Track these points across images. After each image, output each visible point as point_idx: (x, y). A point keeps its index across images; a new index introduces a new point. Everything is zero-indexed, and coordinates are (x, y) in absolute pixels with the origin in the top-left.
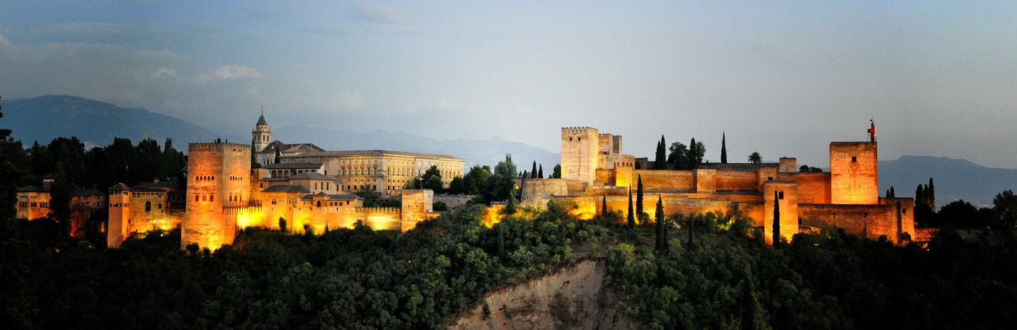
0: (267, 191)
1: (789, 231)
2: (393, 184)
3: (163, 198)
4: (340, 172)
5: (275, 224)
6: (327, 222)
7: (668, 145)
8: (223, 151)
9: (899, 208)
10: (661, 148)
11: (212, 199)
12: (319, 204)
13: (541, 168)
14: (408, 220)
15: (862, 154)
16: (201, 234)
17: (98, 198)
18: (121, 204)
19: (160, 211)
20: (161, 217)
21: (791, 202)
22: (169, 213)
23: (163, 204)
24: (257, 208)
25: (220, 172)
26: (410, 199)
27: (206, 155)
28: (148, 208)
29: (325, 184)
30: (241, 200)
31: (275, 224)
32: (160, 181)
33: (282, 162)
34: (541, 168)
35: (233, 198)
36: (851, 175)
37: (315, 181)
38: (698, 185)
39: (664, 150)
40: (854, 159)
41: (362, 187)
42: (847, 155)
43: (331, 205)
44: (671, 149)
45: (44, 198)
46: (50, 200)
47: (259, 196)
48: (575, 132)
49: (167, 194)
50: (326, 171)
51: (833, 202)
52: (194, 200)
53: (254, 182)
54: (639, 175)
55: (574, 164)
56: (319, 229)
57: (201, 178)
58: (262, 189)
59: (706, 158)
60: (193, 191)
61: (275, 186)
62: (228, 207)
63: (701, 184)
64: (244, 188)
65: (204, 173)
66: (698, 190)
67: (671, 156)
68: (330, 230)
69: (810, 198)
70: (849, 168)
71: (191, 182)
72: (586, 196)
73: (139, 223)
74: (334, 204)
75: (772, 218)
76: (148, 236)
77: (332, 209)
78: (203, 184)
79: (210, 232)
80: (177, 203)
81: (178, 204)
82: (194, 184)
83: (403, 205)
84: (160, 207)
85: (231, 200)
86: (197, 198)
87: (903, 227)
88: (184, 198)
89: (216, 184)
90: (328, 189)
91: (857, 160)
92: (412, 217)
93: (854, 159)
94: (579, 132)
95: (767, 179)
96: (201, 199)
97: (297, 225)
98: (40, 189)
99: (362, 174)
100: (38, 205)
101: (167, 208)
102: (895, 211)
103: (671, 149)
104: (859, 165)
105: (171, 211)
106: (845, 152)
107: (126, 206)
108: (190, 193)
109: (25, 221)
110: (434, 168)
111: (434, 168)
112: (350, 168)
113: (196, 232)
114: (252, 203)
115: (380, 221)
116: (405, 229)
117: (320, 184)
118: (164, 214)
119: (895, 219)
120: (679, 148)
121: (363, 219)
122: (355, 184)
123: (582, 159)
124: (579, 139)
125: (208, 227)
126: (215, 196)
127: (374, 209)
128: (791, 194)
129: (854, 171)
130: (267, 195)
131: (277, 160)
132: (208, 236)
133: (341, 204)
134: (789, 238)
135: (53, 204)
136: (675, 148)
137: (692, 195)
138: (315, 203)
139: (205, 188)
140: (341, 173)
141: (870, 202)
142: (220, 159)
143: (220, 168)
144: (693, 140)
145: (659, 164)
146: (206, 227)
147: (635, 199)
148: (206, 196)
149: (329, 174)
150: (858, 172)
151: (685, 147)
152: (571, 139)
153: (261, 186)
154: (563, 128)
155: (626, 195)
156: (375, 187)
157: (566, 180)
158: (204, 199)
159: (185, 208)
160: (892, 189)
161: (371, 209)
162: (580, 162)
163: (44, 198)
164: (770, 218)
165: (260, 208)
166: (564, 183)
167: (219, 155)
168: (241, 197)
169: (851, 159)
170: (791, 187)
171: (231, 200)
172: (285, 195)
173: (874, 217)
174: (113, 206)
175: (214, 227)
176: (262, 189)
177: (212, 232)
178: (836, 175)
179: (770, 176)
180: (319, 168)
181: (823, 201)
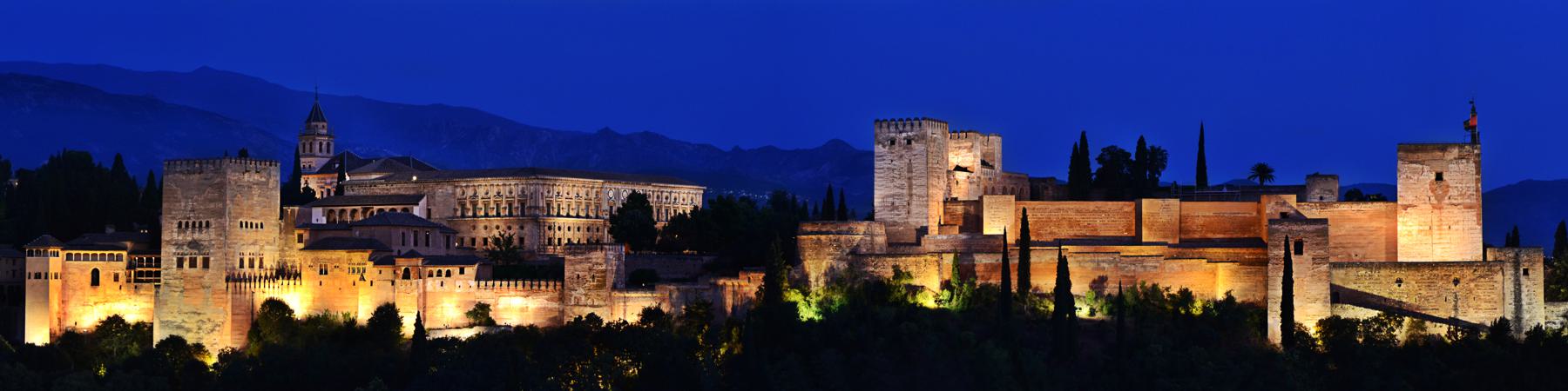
0: (310, 247)
1: (1310, 314)
2: (558, 234)
3: (120, 267)
4: (455, 210)
7: (1094, 153)
8: (225, 173)
9: (1517, 270)
10: (1080, 156)
13: (842, 195)
14: (577, 304)
15: (1453, 166)
17: (14, 264)
18: (47, 275)
19: (117, 285)
20: (118, 298)
21: (1316, 260)
22: (133, 290)
23: (122, 274)
24: (292, 282)
25: (220, 214)
26: (580, 262)
28: (95, 280)
29: (422, 236)
32: (116, 230)
33: (348, 192)
34: (842, 195)
36: (1434, 207)
37: (401, 230)
38: (1145, 232)
39: (1087, 163)
40: (1439, 177)
41: (496, 241)
42: (1426, 168)
43: (431, 275)
44: (1100, 160)
47: (297, 256)
48: (901, 129)
50: (429, 211)
51: (1399, 260)
52: (175, 266)
53: (286, 233)
54: (1024, 210)
55: (898, 191)
57: (187, 224)
58: (302, 246)
59: (1165, 178)
61: (328, 239)
63: (1150, 229)
66: (1144, 240)
67: (1099, 172)
69: (1358, 250)
70: (1430, 194)
72: (919, 254)
73: (81, 309)
74: (435, 274)
75: (1280, 293)
79: (204, 327)
81: (149, 274)
83: (567, 274)
84: (116, 278)
86: (180, 264)
87: (1524, 303)
88: (158, 261)
89: (213, 236)
90: (427, 244)
91: (1445, 177)
92: (583, 298)
93: (1439, 177)
94: (908, 128)
95: (1278, 217)
96: (186, 264)
99: (498, 215)
101: (128, 281)
102: (1509, 272)
103: (1100, 160)
104: (1448, 186)
105: (136, 287)
106: (1422, 163)
107: (56, 277)
112: (474, 204)
114: (284, 273)
117: (412, 235)
118: (123, 292)
119: (1510, 286)
120: (1113, 156)
123: (914, 182)
124: (909, 142)
125: (201, 317)
126: (212, 259)
128: (1317, 244)
129: (1440, 199)
130: (310, 256)
131: (340, 190)
132: (202, 334)
133: (448, 274)
134: (1313, 330)
136: (1108, 157)
137: (1133, 250)
138: (401, 272)
139: (194, 244)
140: (459, 213)
141: (1468, 258)
142: (221, 187)
143: (221, 205)
144: (1141, 142)
145: (1080, 187)
146: (198, 318)
147: (1014, 261)
148: (196, 259)
149: (435, 216)
150: (1447, 201)
151: (1129, 155)
152: (893, 143)
153: (300, 241)
154: (877, 121)
155: (999, 252)
156: (521, 240)
157: (882, 222)
159: (159, 281)
160: (1515, 231)
162: (910, 187)
164: (1277, 292)
165: (298, 283)
166: (879, 230)
167: (219, 180)
169: (1433, 177)
170: (1317, 231)
172: (342, 254)
173: (1472, 285)
174: (32, 277)
175: (209, 315)
176: (302, 246)
177: (209, 326)
178: (1406, 207)
179: (1284, 209)
180: (418, 204)
181: (1382, 258)
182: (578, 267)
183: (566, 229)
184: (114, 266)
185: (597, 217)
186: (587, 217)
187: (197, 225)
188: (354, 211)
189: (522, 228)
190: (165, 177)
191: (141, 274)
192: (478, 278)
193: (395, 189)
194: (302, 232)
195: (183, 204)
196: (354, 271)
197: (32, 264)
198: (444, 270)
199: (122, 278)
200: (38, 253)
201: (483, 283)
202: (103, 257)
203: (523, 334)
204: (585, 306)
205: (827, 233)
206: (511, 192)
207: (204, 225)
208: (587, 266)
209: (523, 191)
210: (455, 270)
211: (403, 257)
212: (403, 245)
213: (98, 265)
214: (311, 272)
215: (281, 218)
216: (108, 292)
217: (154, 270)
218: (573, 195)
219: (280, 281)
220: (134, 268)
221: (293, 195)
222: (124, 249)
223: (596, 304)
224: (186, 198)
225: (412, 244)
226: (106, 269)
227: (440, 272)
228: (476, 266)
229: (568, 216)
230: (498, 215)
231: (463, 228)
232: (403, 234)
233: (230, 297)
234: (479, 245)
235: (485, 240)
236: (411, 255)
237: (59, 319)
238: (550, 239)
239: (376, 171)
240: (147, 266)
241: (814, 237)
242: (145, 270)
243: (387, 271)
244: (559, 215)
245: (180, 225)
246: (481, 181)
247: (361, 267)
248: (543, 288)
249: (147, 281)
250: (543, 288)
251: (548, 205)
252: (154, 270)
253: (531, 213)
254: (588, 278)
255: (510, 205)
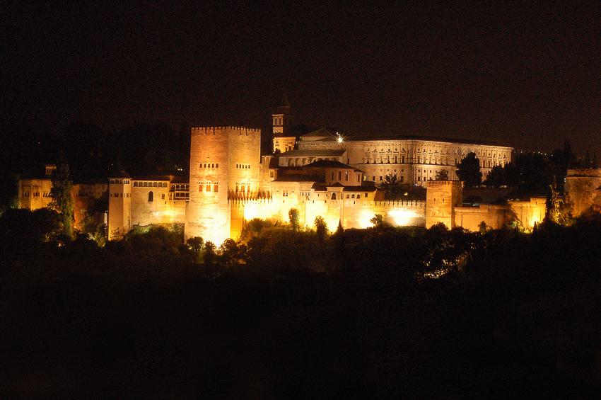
2: (424, 175)
3: (166, 191)
5: (286, 220)
6: (342, 216)
11: (216, 190)
12: (334, 197)
14: (434, 216)
16: (205, 228)
19: (163, 201)
23: (167, 194)
24: (267, 200)
27: (211, 140)
30: (248, 191)
31: (286, 220)
33: (301, 148)
35: (240, 188)
41: (387, 178)
43: (348, 197)
45: (46, 187)
46: (52, 189)
47: (270, 185)
49: (171, 182)
56: (332, 228)
60: (197, 180)
62: (233, 197)
64: (253, 177)
65: (208, 160)
68: (345, 227)
71: (195, 170)
74: (351, 197)
76: (151, 229)
77: (349, 203)
78: (208, 172)
80: (182, 191)
81: (182, 195)
82: (198, 172)
83: (428, 198)
84: (163, 196)
85: (237, 191)
86: (201, 190)
88: (188, 187)
89: (220, 173)
97: (307, 223)
98: (42, 176)
100: (41, 195)
108: (194, 182)
109: (26, 211)
110: (472, 155)
111: (472, 155)
112: (374, 156)
113: (200, 226)
114: (261, 195)
115: (402, 215)
116: (428, 226)
117: (338, 174)
121: (383, 214)
122: (381, 174)
126: (219, 186)
127: (396, 203)
131: (296, 147)
133: (358, 197)
135: (55, 193)
138: (330, 196)
139: (209, 177)
156: (402, 177)
158: (208, 189)
159: (188, 199)
161: (391, 203)
163: (46, 187)
165: (270, 200)
168: (249, 187)
171: (237, 191)
176: (273, 179)
182: (435, 194)
183: (428, 170)
184: (162, 190)
185: (447, 165)
186: (442, 164)
187: (211, 166)
188: (304, 159)
189: (402, 171)
190: (192, 137)
191: (178, 195)
192: (376, 199)
193: (328, 146)
194: (273, 171)
195: (203, 153)
196: (303, 194)
197: (113, 189)
198: (356, 194)
199: (167, 197)
200: (117, 182)
201: (378, 202)
202: (155, 185)
203: (403, 233)
204: (439, 217)
205: (584, 176)
206: (396, 150)
207: (215, 166)
208: (441, 193)
209: (403, 149)
210: (362, 194)
211: (332, 186)
212: (333, 179)
213: (153, 189)
214: (278, 195)
215: (261, 163)
216: (158, 205)
217: (185, 192)
218: (433, 151)
219: (260, 200)
220: (174, 191)
221: (266, 148)
222: (168, 180)
223: (445, 216)
224: (205, 150)
225: (338, 178)
226: (157, 192)
227: (353, 195)
228: (375, 192)
229: (430, 164)
230: (389, 163)
231: (368, 170)
232: (333, 174)
233: (230, 209)
234: (377, 181)
235: (381, 177)
236: (337, 185)
237: (129, 221)
238: (419, 178)
239: (317, 135)
240: (182, 190)
241: (576, 178)
242: (180, 192)
243: (322, 194)
244: (424, 163)
245: (201, 166)
246: (380, 142)
247: (308, 192)
248: (414, 206)
249: (181, 199)
250: (414, 206)
251: (419, 157)
252: (185, 192)
253: (409, 161)
254: (441, 201)
255: (396, 157)
